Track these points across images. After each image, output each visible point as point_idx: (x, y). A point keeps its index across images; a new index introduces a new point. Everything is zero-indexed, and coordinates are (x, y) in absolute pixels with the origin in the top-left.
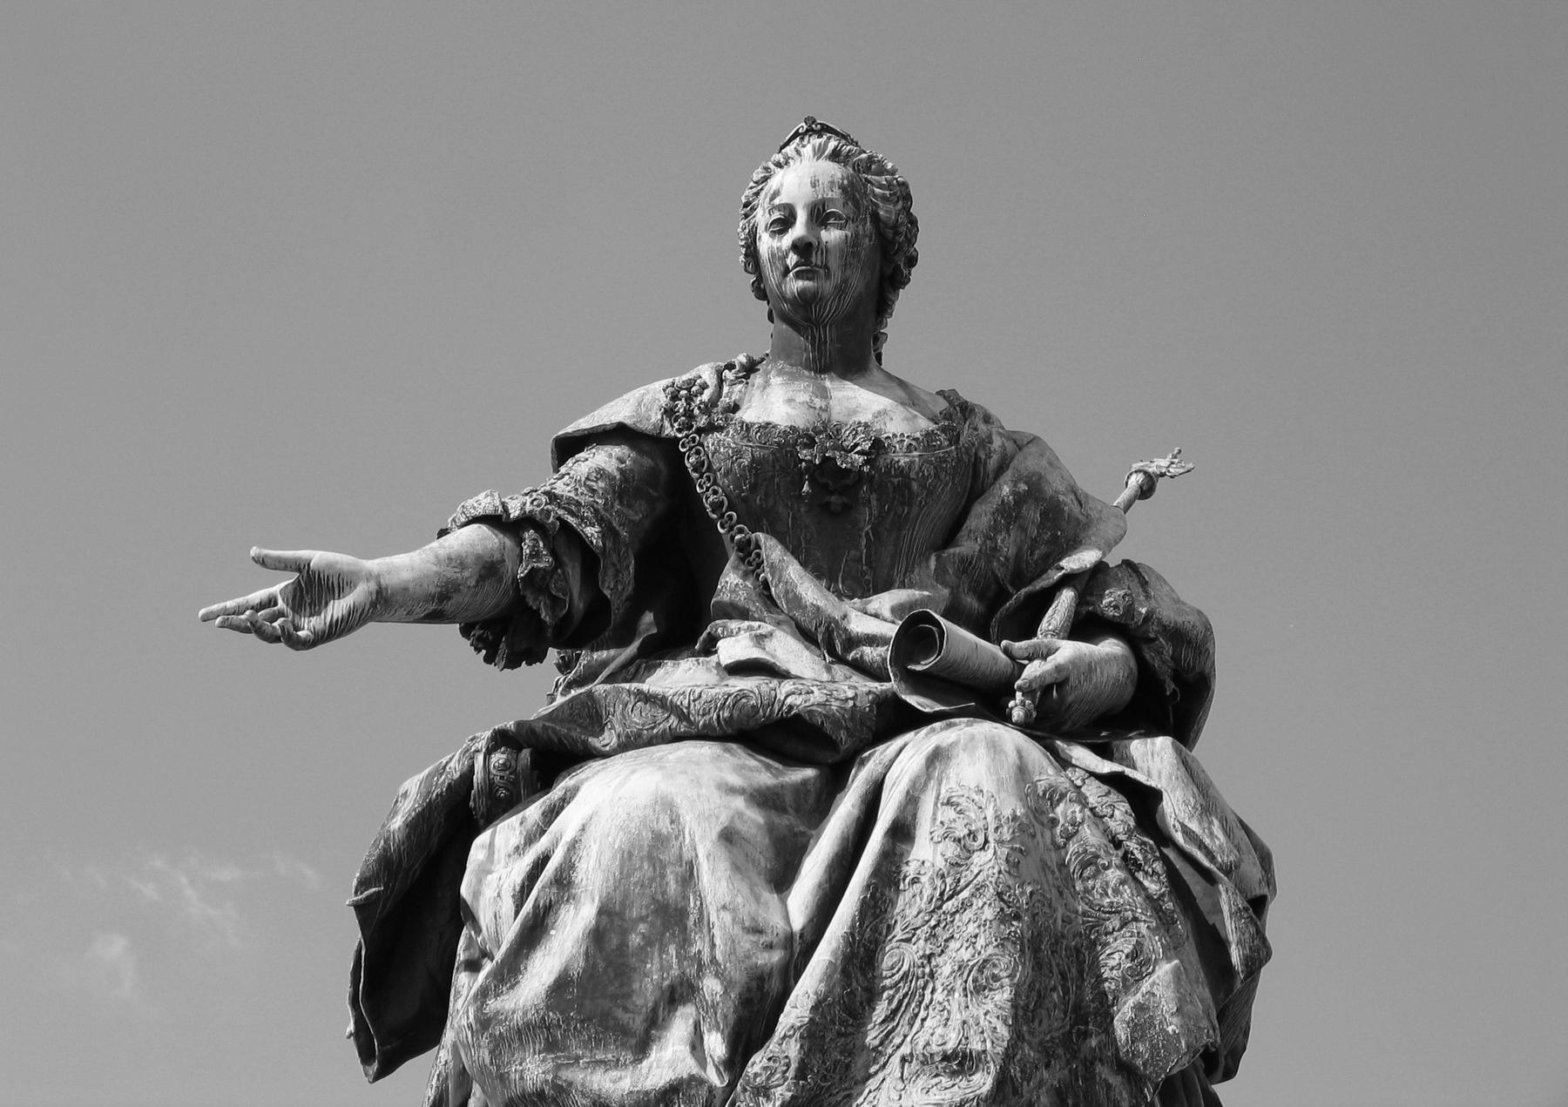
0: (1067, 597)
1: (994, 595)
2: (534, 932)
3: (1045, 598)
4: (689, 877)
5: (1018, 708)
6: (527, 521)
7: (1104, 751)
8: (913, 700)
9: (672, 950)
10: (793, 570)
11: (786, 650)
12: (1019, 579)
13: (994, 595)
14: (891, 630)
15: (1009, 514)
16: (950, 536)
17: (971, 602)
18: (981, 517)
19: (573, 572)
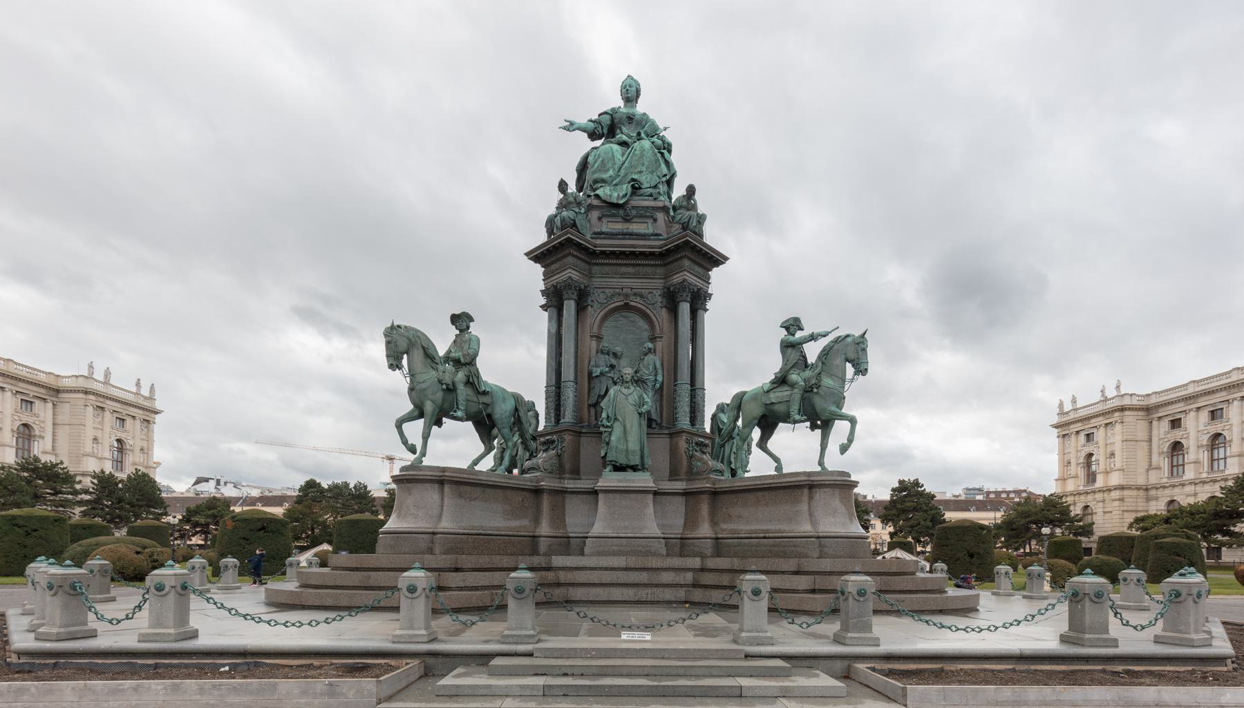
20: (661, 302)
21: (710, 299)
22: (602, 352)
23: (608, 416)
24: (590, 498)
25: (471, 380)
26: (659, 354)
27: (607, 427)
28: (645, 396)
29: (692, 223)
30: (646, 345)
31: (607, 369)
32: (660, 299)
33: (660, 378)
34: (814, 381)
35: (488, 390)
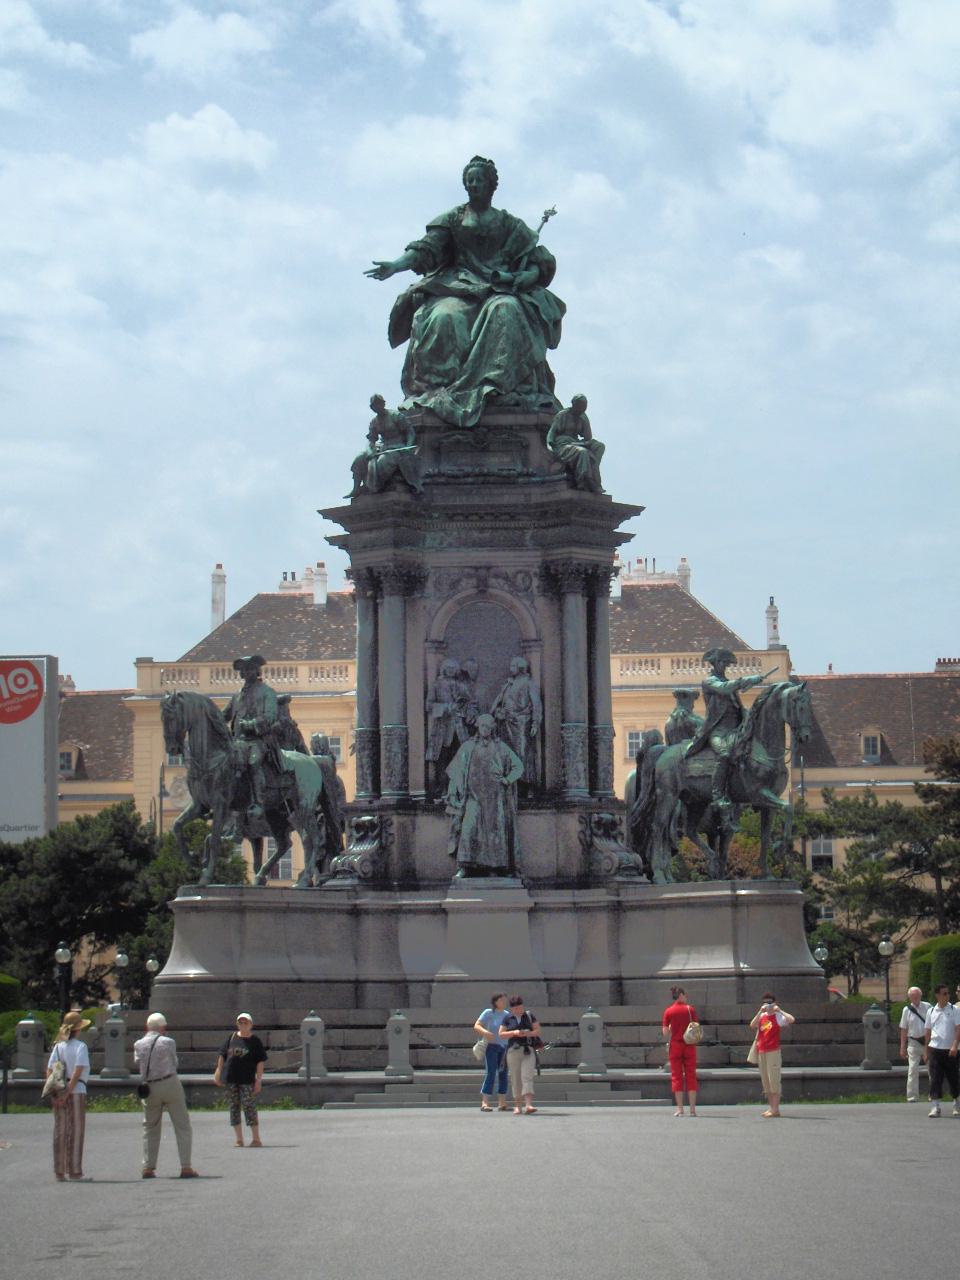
0: (525, 259)
1: (510, 255)
2: (427, 338)
3: (521, 259)
4: (453, 330)
5: (514, 289)
6: (422, 249)
7: (530, 294)
8: (494, 288)
9: (450, 344)
10: (473, 257)
11: (472, 278)
12: (517, 252)
13: (510, 255)
14: (491, 272)
15: (515, 240)
16: (503, 246)
17: (507, 259)
18: (510, 241)
19: (431, 259)
20: (538, 587)
21: (616, 575)
22: (445, 672)
23: (458, 794)
24: (441, 916)
25: (270, 760)
26: (536, 671)
27: (456, 808)
28: (513, 755)
29: (581, 467)
30: (513, 662)
31: (455, 706)
32: (536, 582)
33: (537, 717)
34: (739, 753)
35: (291, 769)
